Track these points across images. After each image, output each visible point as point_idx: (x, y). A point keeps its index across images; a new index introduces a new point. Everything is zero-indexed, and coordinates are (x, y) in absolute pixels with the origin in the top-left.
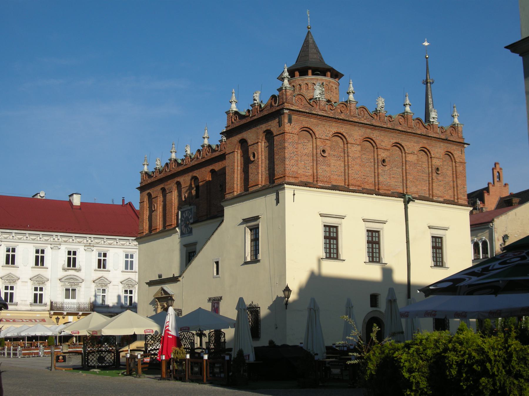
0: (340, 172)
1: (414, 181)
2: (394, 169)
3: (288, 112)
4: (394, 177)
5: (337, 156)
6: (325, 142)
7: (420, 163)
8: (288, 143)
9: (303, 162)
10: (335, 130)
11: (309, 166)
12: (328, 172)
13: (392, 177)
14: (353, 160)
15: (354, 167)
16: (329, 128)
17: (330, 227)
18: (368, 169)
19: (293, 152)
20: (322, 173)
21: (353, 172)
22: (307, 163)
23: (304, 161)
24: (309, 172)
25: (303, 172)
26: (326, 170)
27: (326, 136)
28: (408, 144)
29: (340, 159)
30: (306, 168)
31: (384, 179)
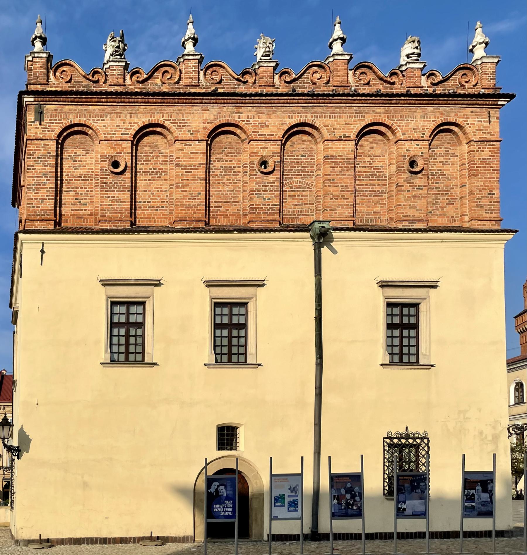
0: (158, 202)
1: (344, 196)
2: (294, 179)
3: (32, 99)
4: (295, 196)
5: (153, 172)
6: (121, 145)
7: (368, 159)
8: (33, 158)
9: (72, 193)
10: (144, 120)
11: (86, 199)
12: (125, 202)
13: (289, 196)
14: (186, 172)
15: (188, 185)
16: (131, 117)
17: (402, 305)
18: (227, 188)
19: (43, 174)
20: (110, 205)
21: (186, 196)
22: (81, 194)
23: (74, 191)
24: (85, 210)
25: (72, 210)
26: (120, 199)
27: (122, 134)
28: (329, 121)
29: (160, 177)
30: (80, 202)
31: (265, 199)
